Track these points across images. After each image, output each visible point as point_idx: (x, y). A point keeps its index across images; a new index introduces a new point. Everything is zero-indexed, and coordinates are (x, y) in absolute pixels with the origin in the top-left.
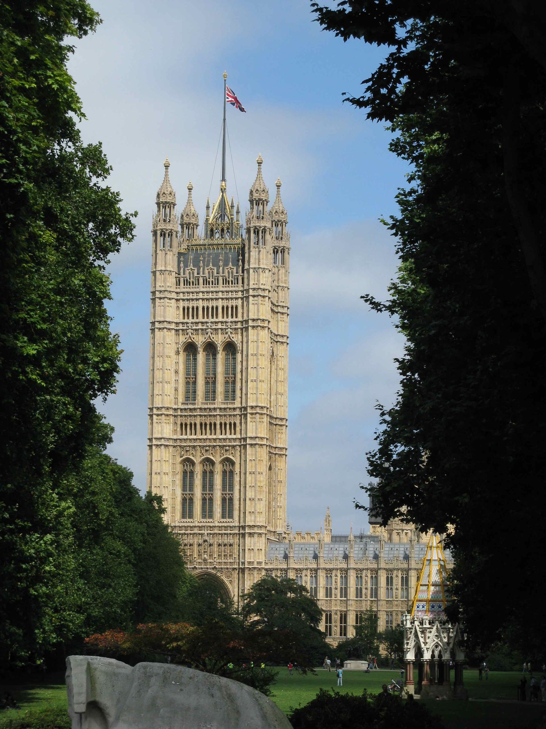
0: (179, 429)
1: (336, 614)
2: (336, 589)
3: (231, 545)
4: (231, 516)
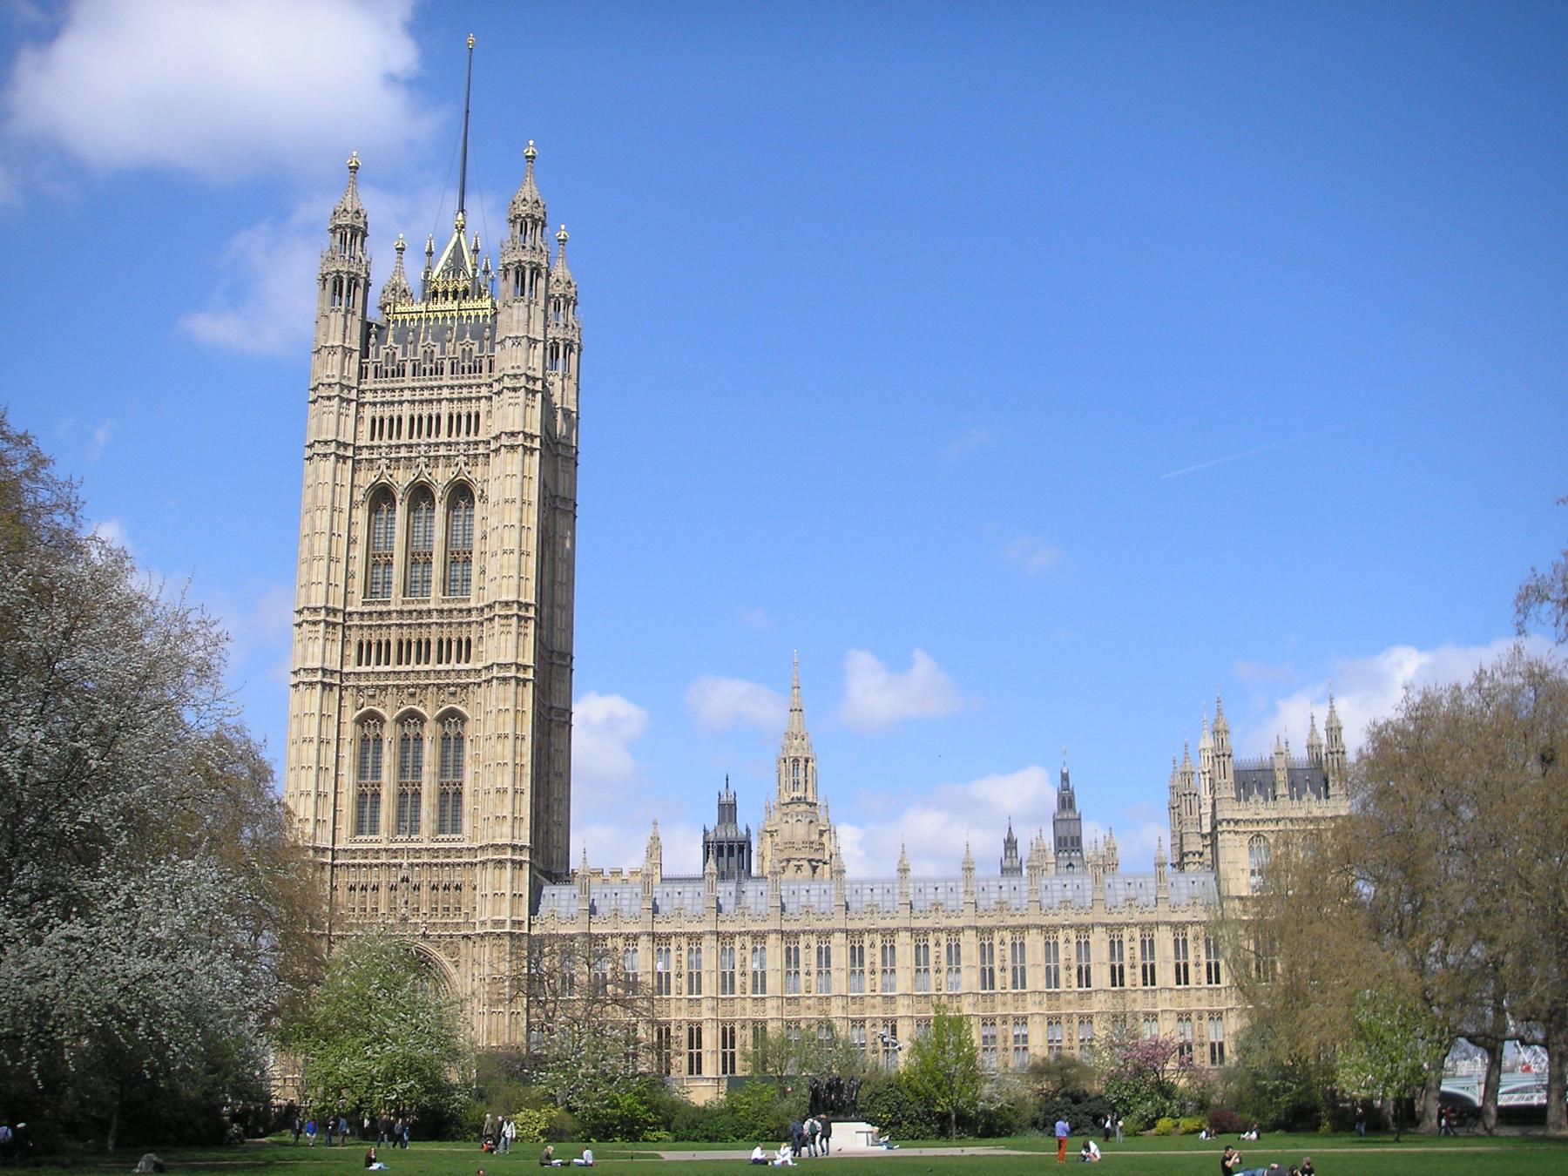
0: (352, 651)
1: (679, 1028)
2: (679, 975)
3: (458, 888)
4: (456, 829)
